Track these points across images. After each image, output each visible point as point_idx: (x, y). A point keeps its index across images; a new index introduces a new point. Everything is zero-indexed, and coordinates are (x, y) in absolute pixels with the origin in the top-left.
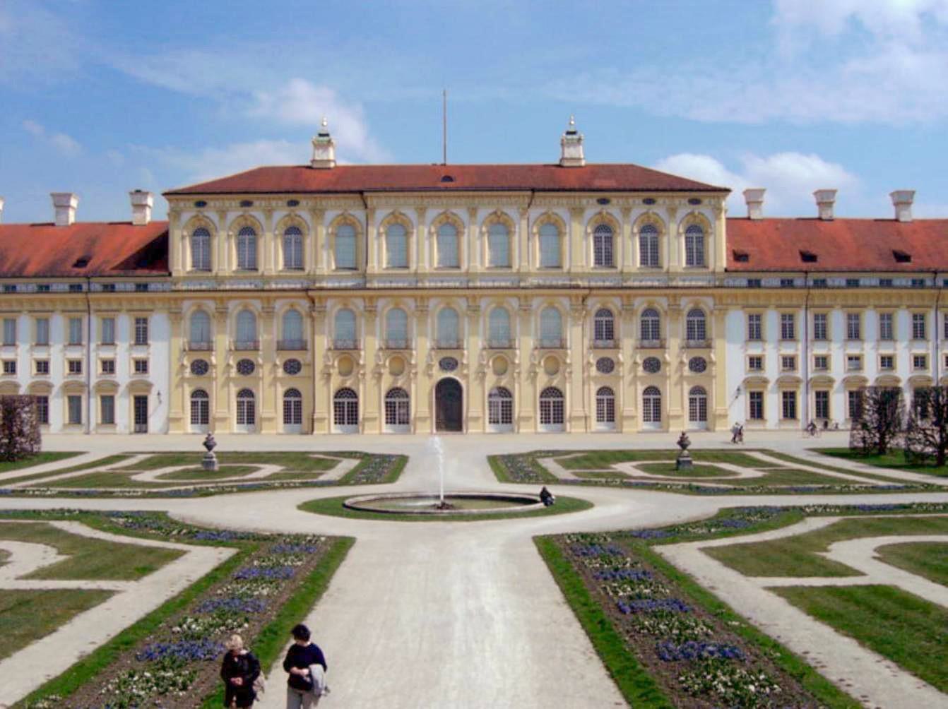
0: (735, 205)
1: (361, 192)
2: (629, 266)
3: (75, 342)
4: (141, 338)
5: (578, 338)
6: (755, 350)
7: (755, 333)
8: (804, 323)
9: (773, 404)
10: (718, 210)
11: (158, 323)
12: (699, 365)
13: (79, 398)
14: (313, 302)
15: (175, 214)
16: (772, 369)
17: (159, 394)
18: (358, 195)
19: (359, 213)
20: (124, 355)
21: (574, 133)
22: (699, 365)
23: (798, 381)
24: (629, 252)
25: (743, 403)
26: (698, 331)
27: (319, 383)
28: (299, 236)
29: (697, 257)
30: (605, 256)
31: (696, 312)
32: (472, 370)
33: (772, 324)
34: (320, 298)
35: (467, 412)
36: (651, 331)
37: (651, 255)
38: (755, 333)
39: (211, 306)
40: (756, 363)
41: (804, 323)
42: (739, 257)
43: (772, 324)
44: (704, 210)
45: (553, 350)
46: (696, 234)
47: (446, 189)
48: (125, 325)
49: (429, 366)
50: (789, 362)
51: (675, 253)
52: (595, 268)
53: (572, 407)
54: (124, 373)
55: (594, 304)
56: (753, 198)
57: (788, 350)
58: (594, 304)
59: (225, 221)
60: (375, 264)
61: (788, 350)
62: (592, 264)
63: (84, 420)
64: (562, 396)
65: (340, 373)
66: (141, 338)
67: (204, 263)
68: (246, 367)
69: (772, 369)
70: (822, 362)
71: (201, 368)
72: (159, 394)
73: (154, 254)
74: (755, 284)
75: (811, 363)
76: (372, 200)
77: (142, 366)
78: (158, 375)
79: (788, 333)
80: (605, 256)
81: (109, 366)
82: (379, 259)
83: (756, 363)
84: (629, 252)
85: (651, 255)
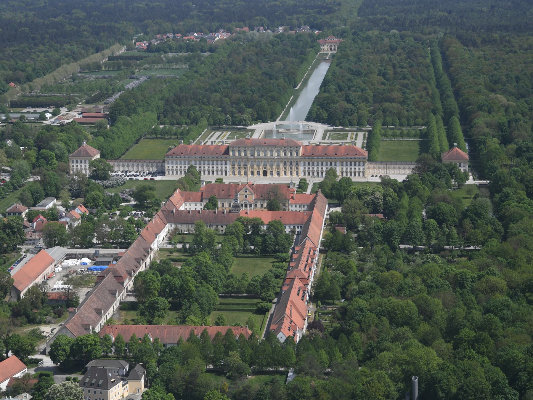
3: (217, 164)
4: (226, 164)
5: (281, 165)
7: (305, 164)
9: (307, 173)
11: (228, 162)
12: (297, 168)
22: (297, 168)
24: (288, 154)
25: (303, 173)
26: (297, 164)
30: (285, 154)
36: (291, 164)
37: (291, 154)
38: (305, 164)
45: (278, 166)
48: (224, 162)
51: (294, 154)
54: (224, 168)
58: (284, 160)
66: (226, 164)
68: (239, 168)
73: (227, 152)
79: (309, 165)
80: (285, 154)
82: (256, 155)
83: (305, 168)
84: (288, 154)
85: (291, 154)
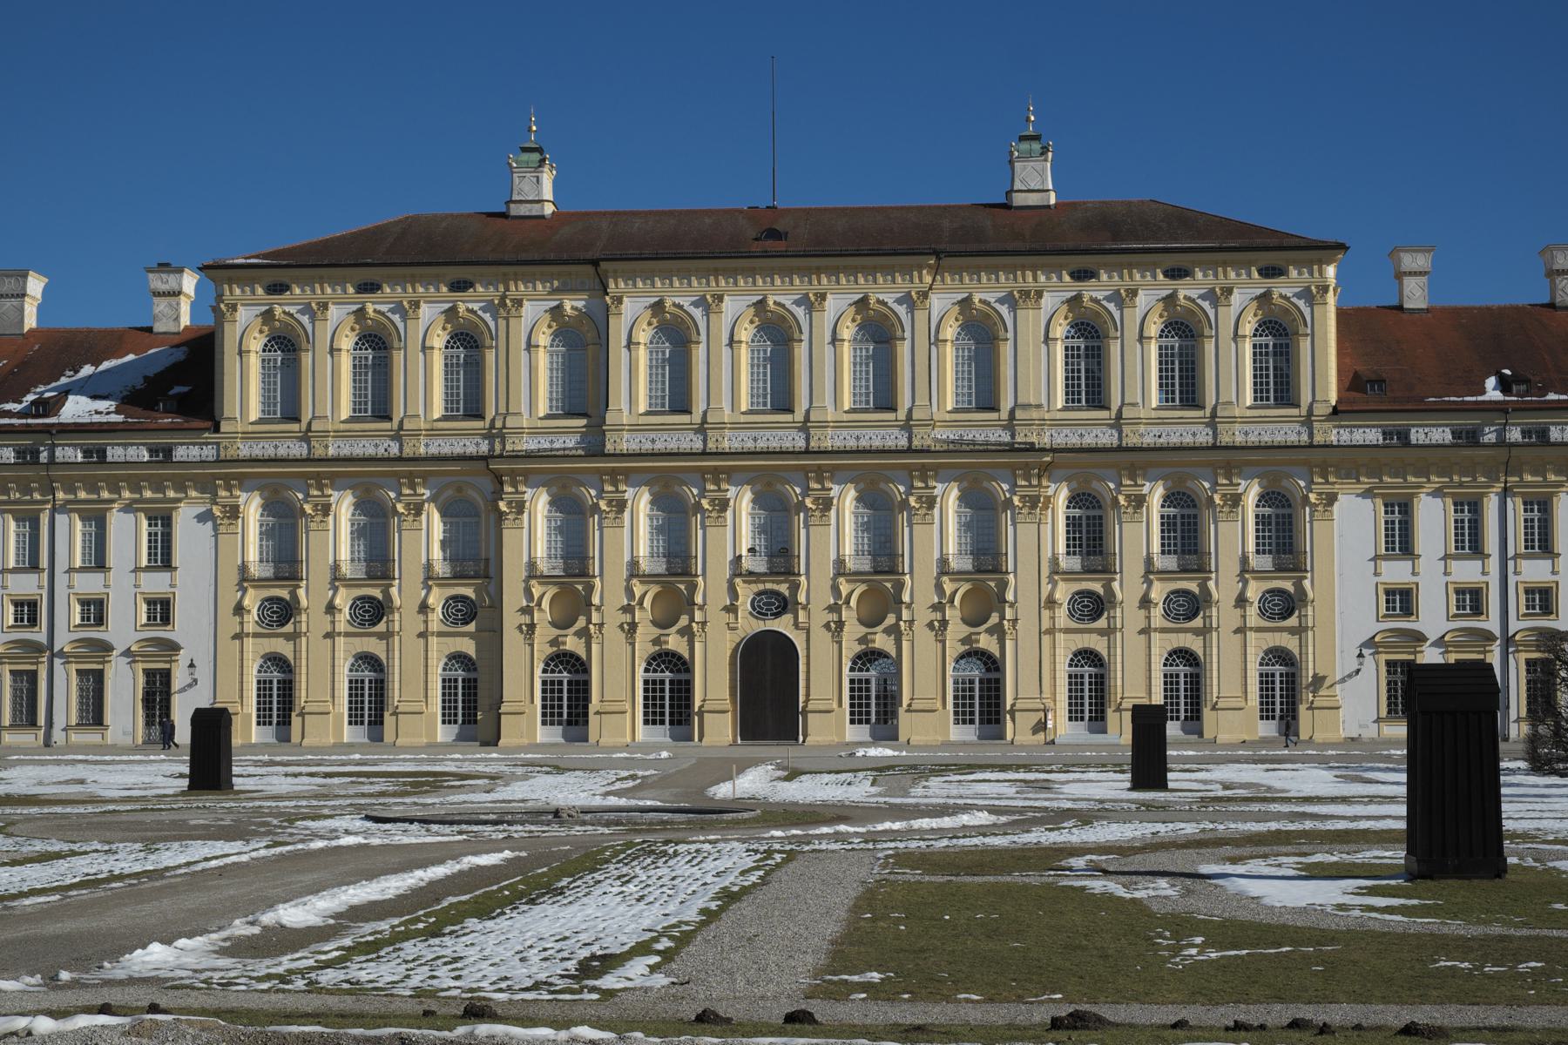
1: (595, 263)
2: (1134, 405)
6: (1397, 572)
7: (1401, 541)
13: (33, 676)
14: (501, 483)
17: (192, 665)
18: (589, 269)
21: (1036, 138)
22: (1284, 606)
23: (1488, 637)
27: (512, 640)
28: (473, 352)
29: (1279, 383)
32: (820, 617)
33: (1433, 518)
34: (513, 474)
35: (807, 700)
36: (1186, 536)
38: (1401, 541)
40: (1402, 600)
43: (1433, 518)
47: (766, 255)
48: (127, 533)
49: (731, 609)
50: (1471, 599)
52: (1065, 409)
54: (125, 626)
57: (1467, 572)
60: (625, 406)
61: (1467, 572)
62: (1060, 402)
63: (42, 720)
64: (997, 669)
65: (554, 624)
66: (162, 556)
67: (287, 403)
72: (192, 665)
73: (182, 384)
75: (1517, 602)
79: (1470, 541)
81: (95, 610)
85: (1184, 382)
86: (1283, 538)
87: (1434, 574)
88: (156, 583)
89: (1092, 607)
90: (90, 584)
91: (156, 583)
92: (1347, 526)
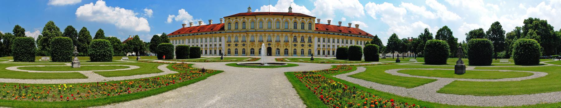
0: (316, 20)
3: (211, 42)
6: (319, 43)
7: (319, 41)
8: (326, 40)
10: (314, 21)
11: (223, 38)
15: (225, 21)
16: (321, 47)
19: (255, 19)
20: (218, 43)
22: (310, 46)
26: (310, 41)
31: (310, 37)
32: (274, 45)
38: (319, 41)
39: (231, 35)
40: (319, 46)
41: (326, 40)
42: (317, 29)
44: (312, 20)
46: (310, 24)
48: (218, 39)
50: (324, 46)
53: (290, 51)
54: (218, 46)
55: (293, 35)
56: (319, 20)
59: (233, 21)
61: (324, 44)
66: (220, 41)
69: (321, 47)
70: (329, 46)
71: (229, 45)
74: (319, 33)
76: (257, 17)
77: (220, 45)
78: (223, 46)
79: (324, 41)
81: (215, 45)
83: (319, 46)
86: (310, 41)
87: (321, 44)
88: (220, 43)
89: (295, 45)
90: (215, 43)
91: (220, 43)
92: (315, 40)
